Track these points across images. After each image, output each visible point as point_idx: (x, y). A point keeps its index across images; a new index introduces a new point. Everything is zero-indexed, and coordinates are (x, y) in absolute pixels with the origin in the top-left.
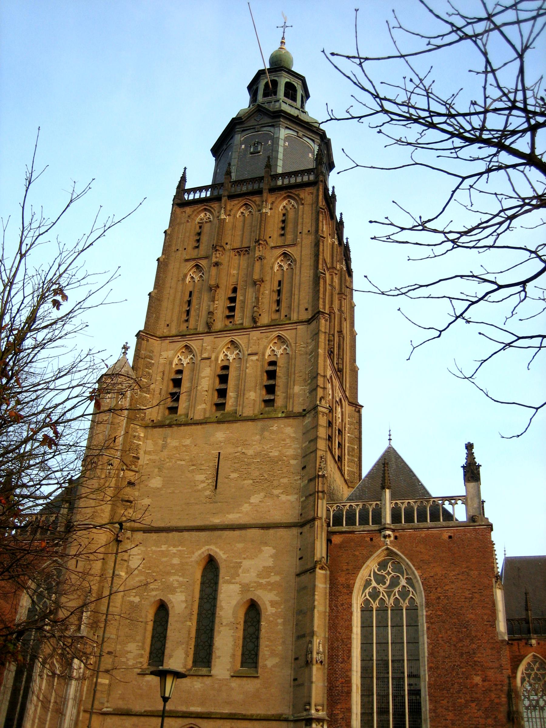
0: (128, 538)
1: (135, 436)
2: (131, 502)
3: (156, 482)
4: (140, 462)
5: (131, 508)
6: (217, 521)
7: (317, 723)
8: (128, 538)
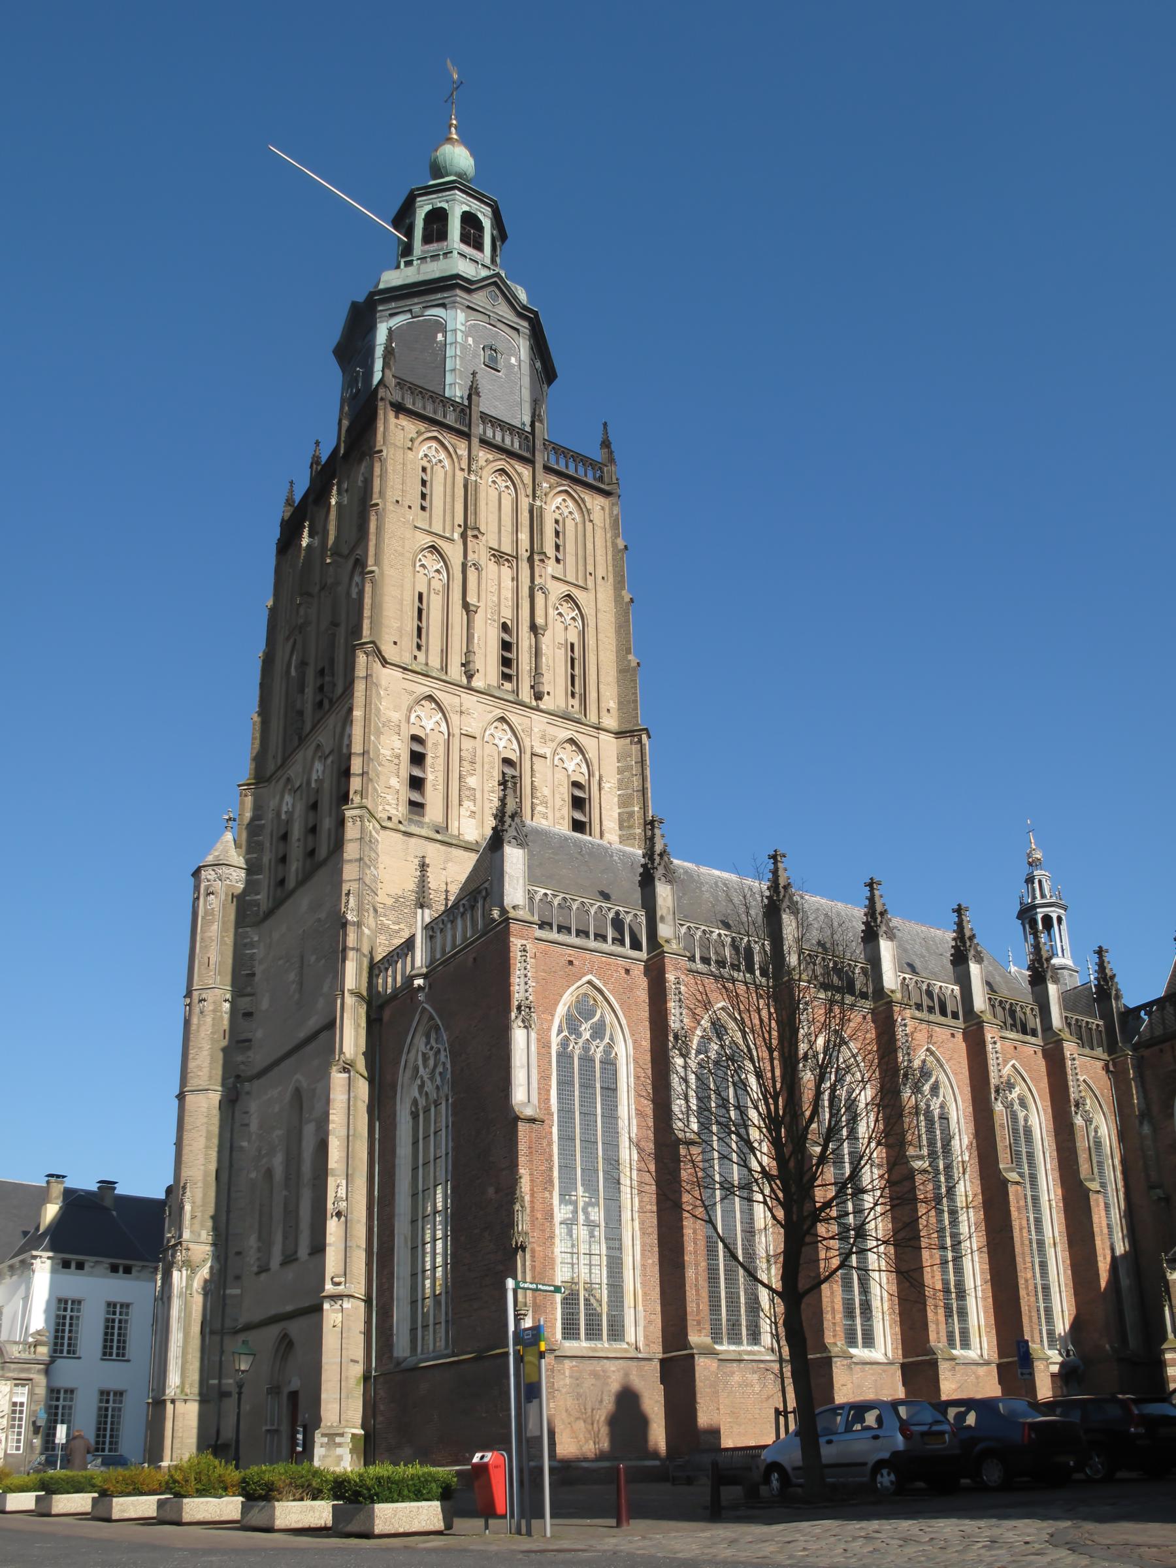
0: (248, 1093)
1: (245, 945)
2: (249, 1041)
3: (265, 1004)
4: (257, 978)
5: (249, 1048)
6: (302, 1034)
7: (333, 1303)
8: (248, 1093)
